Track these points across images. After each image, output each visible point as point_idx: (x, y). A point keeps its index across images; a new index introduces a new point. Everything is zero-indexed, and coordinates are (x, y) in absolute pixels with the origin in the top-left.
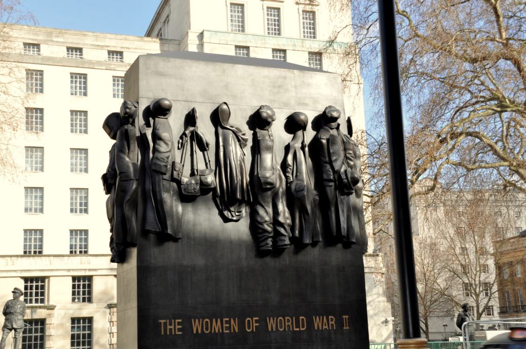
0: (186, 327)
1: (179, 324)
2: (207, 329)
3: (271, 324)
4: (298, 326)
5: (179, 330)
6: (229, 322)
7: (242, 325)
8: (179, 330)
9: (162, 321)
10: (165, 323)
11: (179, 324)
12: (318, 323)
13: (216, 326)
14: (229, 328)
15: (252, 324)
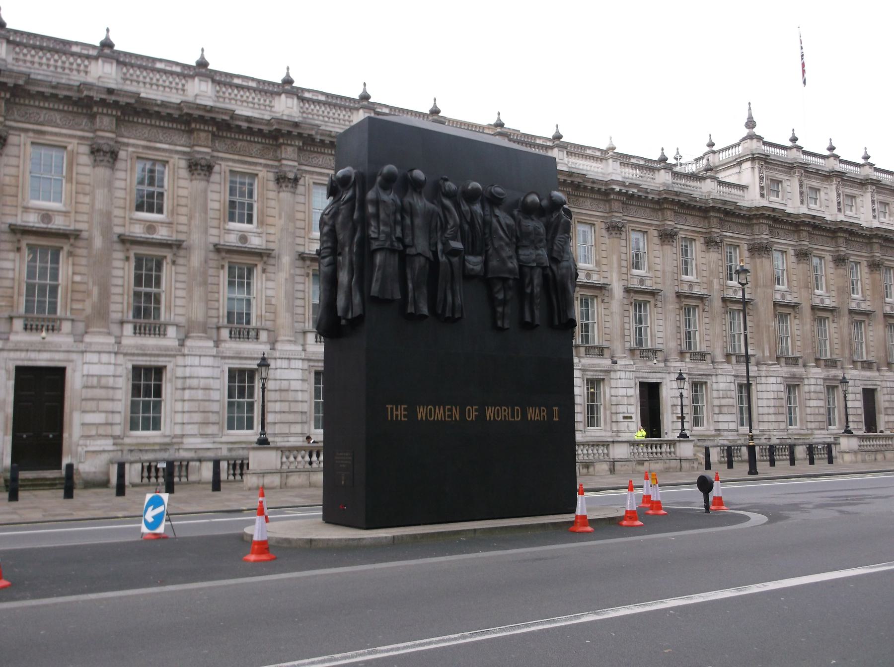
0: (412, 413)
1: (405, 410)
2: (431, 416)
3: (490, 413)
4: (513, 416)
5: (405, 416)
6: (450, 410)
7: (462, 413)
8: (405, 416)
9: (389, 407)
10: (392, 409)
11: (405, 410)
12: (534, 414)
13: (439, 414)
14: (450, 416)
15: (472, 413)
